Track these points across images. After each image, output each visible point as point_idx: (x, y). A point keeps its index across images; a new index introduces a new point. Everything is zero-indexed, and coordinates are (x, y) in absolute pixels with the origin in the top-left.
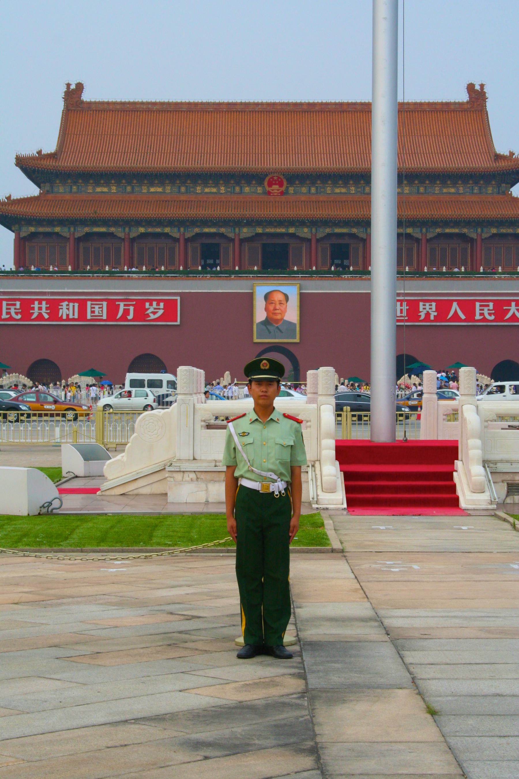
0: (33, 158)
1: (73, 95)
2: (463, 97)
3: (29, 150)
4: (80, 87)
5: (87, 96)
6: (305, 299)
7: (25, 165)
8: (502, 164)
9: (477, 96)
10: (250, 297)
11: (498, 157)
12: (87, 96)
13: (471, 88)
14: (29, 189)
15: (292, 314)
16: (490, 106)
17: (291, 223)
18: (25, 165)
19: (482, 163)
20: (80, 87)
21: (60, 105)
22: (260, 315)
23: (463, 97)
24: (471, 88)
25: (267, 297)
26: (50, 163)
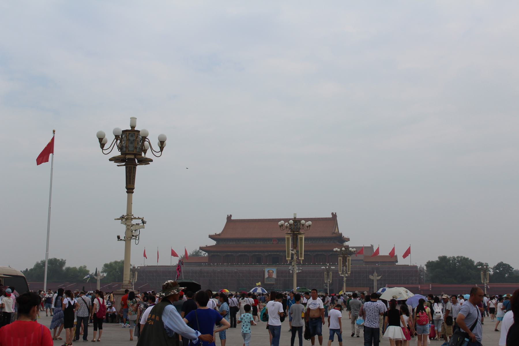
0: (214, 235)
1: (229, 218)
2: (331, 216)
3: (213, 233)
4: (231, 216)
5: (232, 218)
6: (278, 273)
7: (211, 237)
8: (334, 235)
9: (334, 216)
10: (264, 272)
11: (334, 233)
12: (232, 218)
13: (332, 214)
14: (213, 243)
15: (274, 276)
16: (338, 219)
17: (278, 251)
18: (211, 237)
19: (328, 235)
20: (231, 216)
21: (226, 221)
22: (266, 276)
23: (331, 216)
24: (332, 214)
25: (268, 271)
26: (219, 237)
